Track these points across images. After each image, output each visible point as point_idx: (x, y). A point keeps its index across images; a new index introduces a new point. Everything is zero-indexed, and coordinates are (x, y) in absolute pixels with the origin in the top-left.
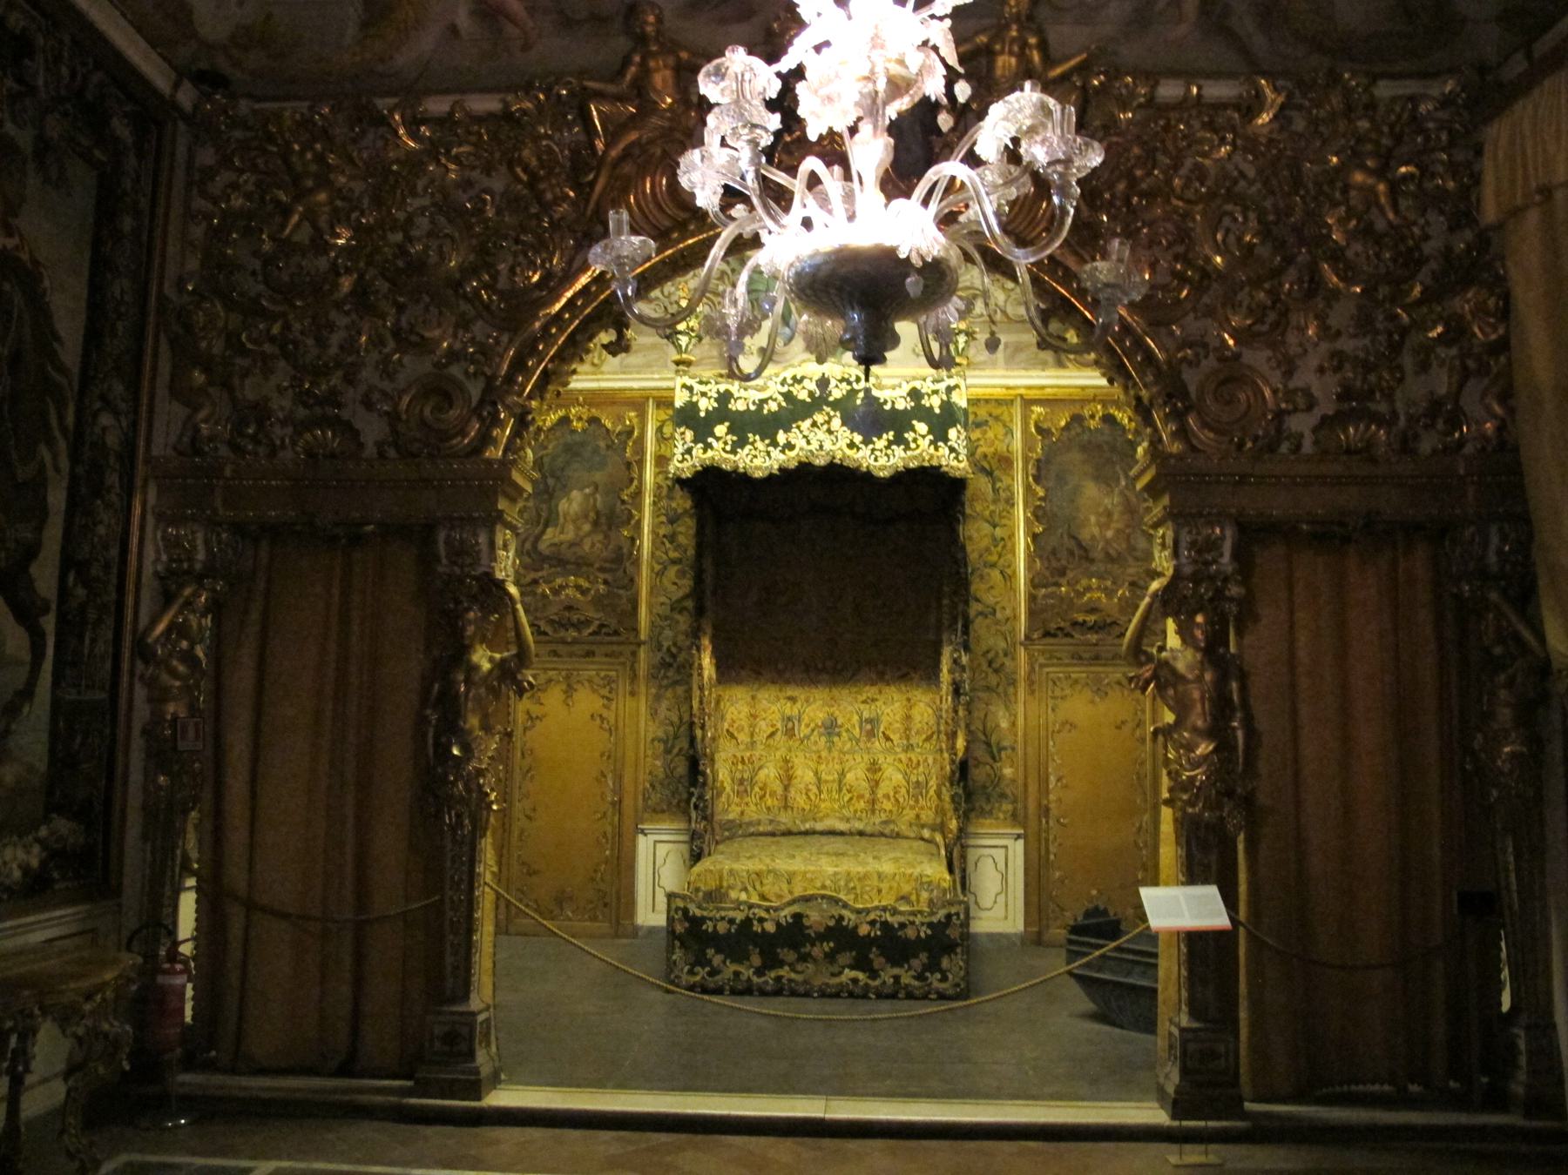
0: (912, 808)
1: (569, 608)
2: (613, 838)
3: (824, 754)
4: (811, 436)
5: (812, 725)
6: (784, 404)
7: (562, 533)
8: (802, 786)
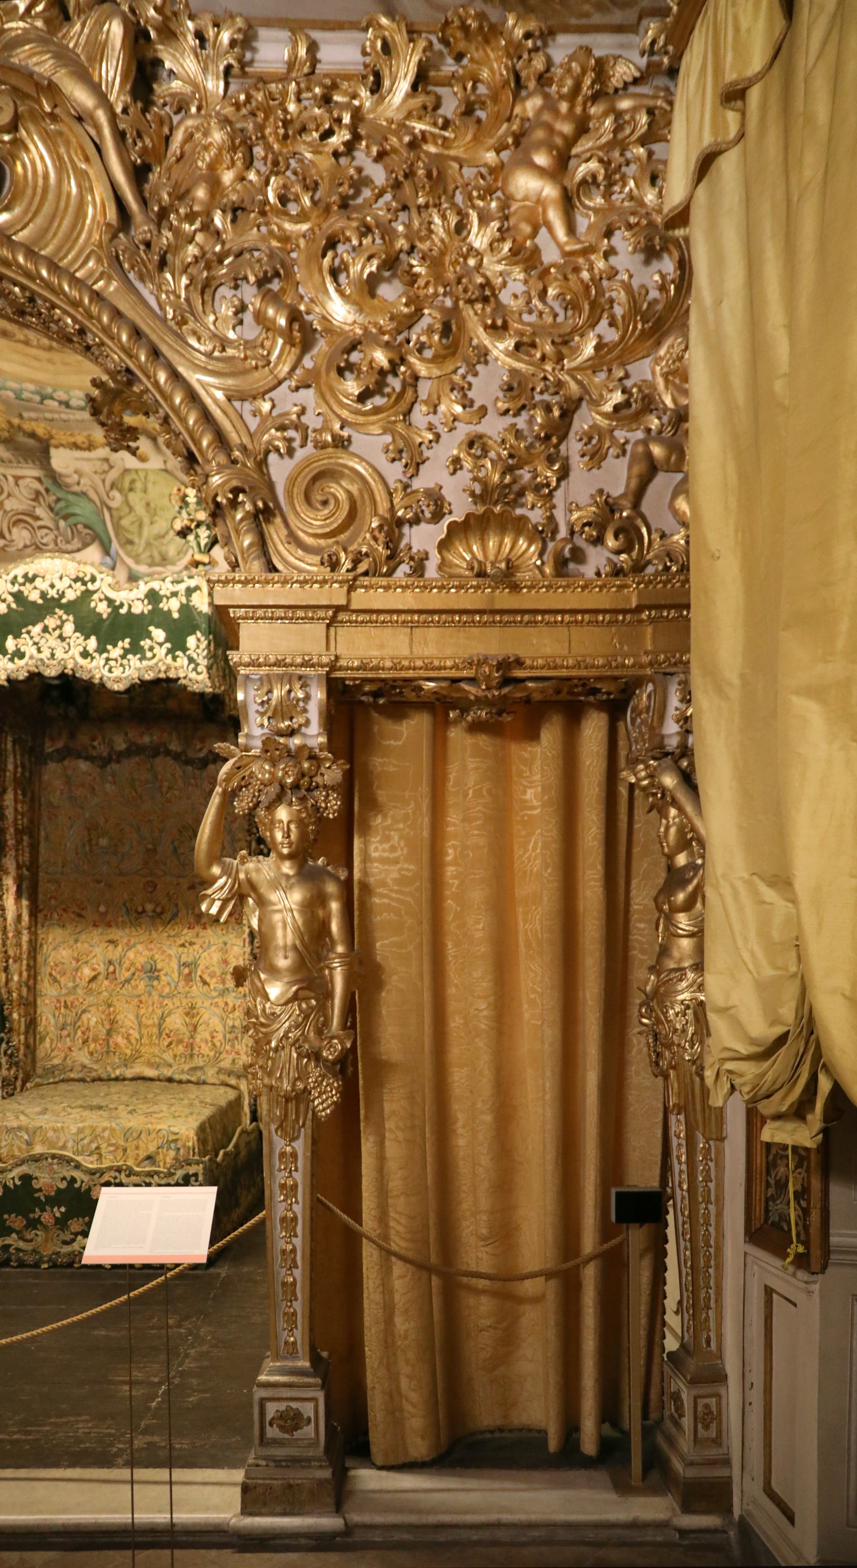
3: (143, 998)
4: (42, 642)
5: (132, 970)
6: (14, 606)
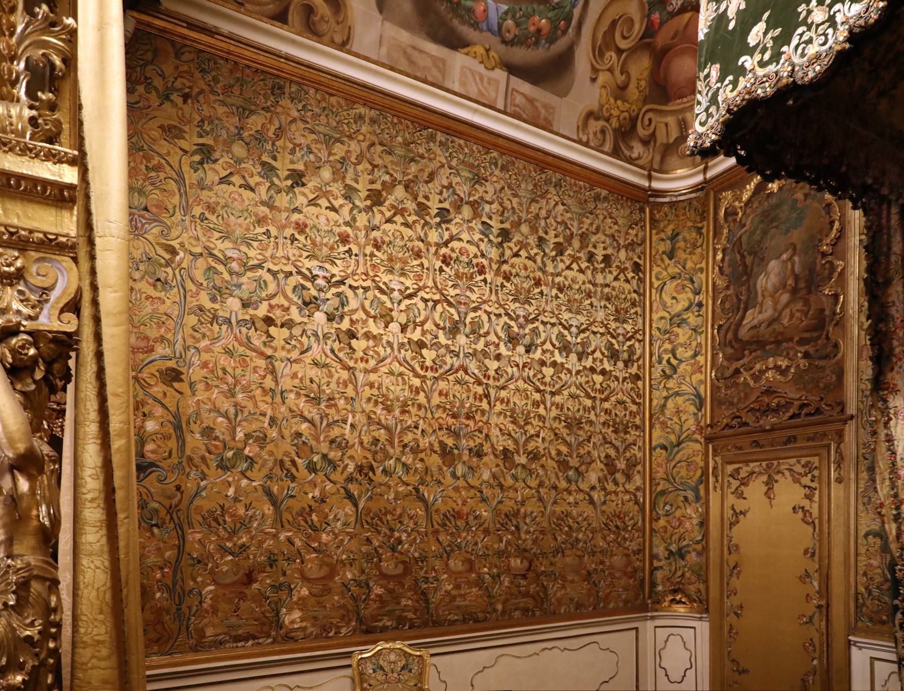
1: (769, 392)
2: (821, 645)
7: (760, 312)
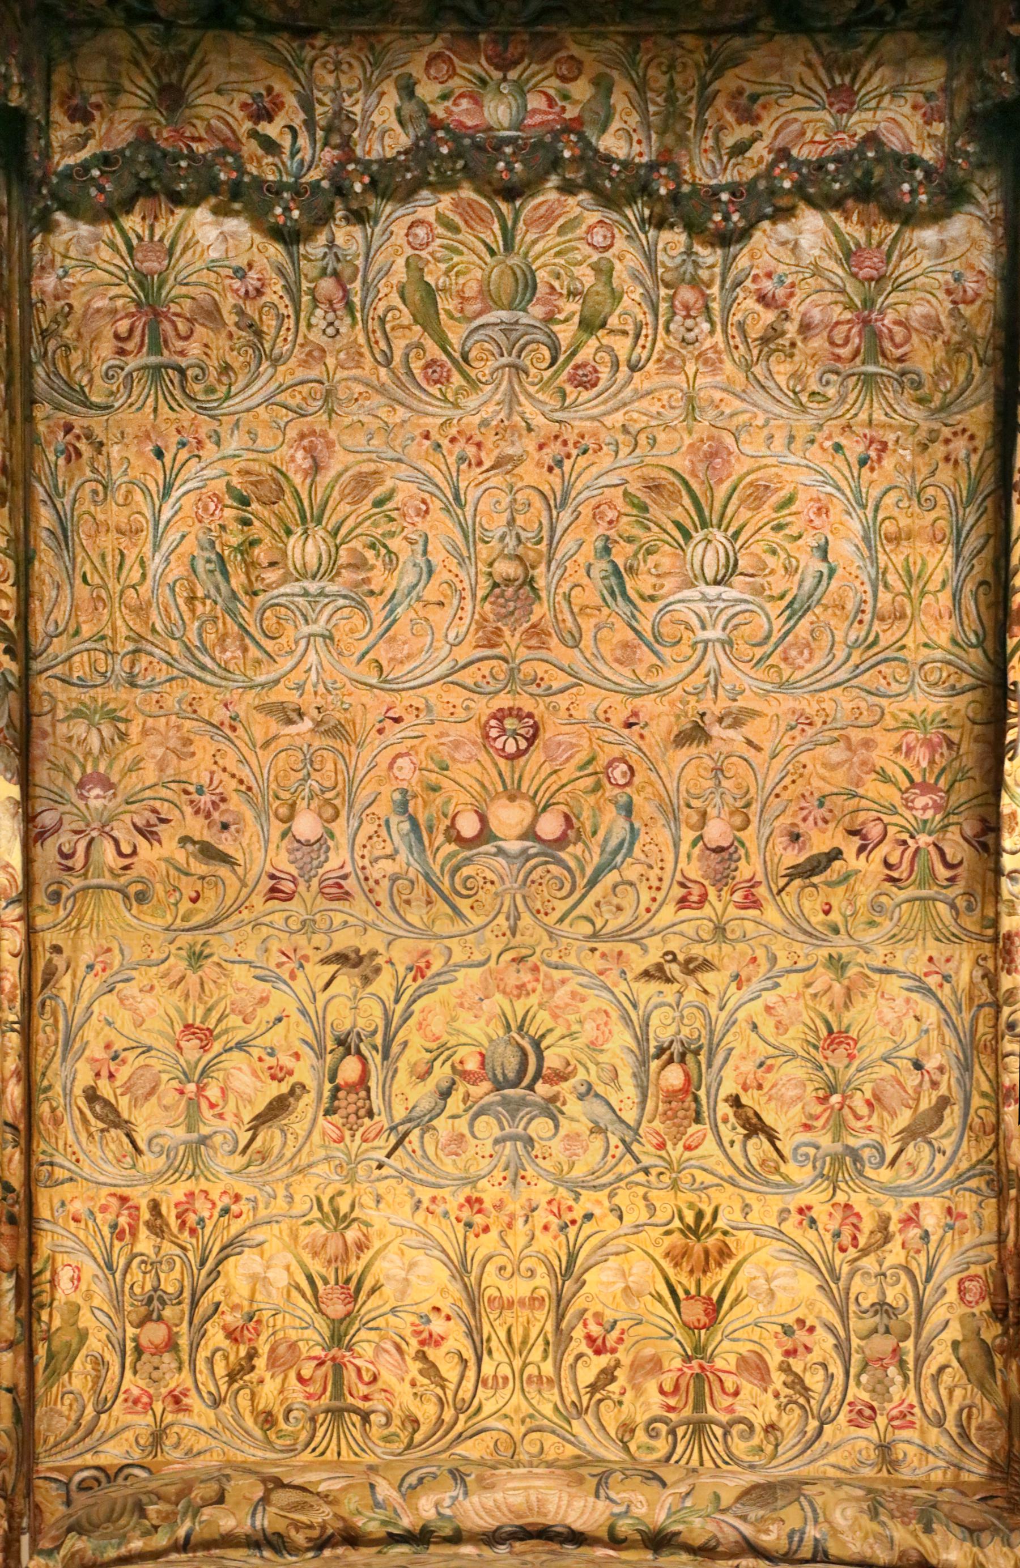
0: (865, 1415)
3: (489, 1192)
5: (442, 1073)
8: (404, 1323)
